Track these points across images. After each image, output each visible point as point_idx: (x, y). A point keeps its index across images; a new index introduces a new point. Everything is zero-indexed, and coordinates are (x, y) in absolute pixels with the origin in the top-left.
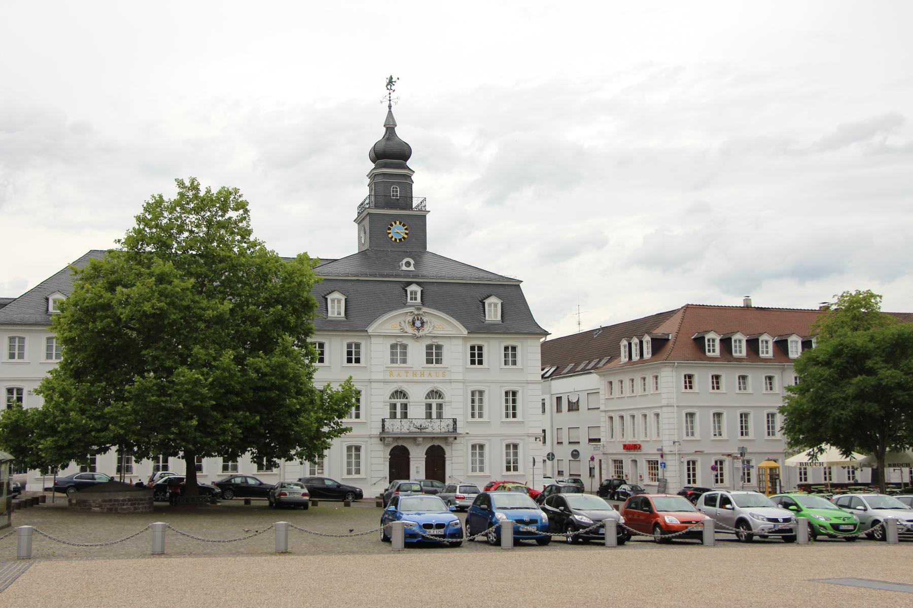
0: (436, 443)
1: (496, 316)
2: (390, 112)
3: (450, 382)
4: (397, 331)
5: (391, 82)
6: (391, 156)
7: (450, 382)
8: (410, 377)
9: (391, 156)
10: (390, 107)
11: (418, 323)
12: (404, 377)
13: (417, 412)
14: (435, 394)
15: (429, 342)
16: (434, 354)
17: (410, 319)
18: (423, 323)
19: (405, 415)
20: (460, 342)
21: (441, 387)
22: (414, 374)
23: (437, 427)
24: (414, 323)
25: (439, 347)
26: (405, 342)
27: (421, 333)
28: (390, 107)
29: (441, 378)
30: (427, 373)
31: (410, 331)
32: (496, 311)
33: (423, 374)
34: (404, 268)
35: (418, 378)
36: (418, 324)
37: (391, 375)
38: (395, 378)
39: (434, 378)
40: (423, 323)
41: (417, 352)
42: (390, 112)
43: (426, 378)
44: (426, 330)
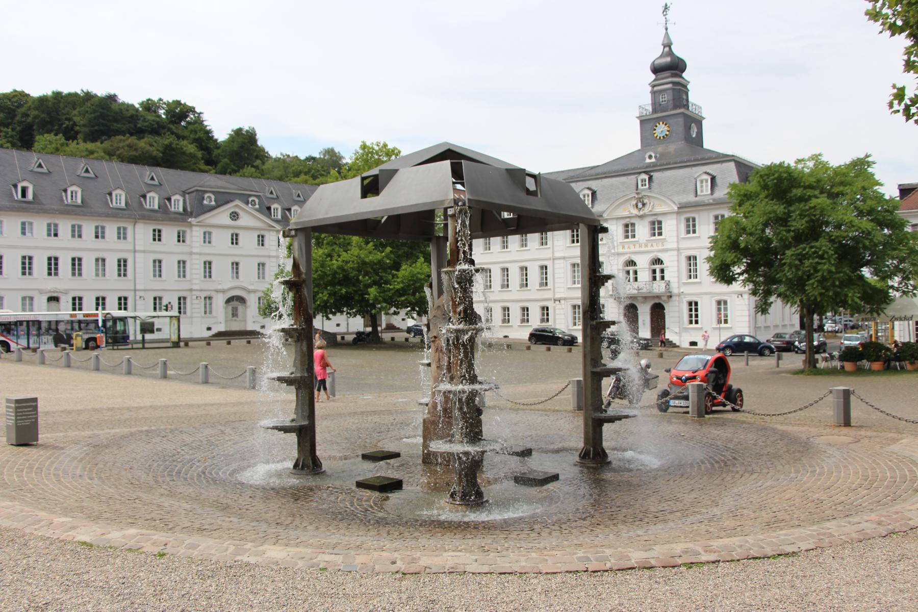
0: (657, 301)
1: (707, 190)
2: (667, 33)
3: (666, 250)
4: (626, 214)
5: (666, 8)
6: (670, 69)
7: (666, 250)
8: (637, 249)
9: (670, 69)
10: (666, 29)
11: (641, 203)
12: (632, 249)
13: (644, 276)
14: (658, 261)
15: (651, 219)
16: (656, 228)
17: (634, 202)
18: (644, 205)
19: (636, 279)
20: (675, 216)
21: (661, 256)
22: (640, 246)
23: (659, 287)
24: (637, 206)
25: (660, 223)
26: (633, 221)
27: (642, 213)
28: (666, 29)
29: (660, 248)
30: (649, 245)
31: (635, 212)
32: (707, 186)
33: (646, 246)
34: (648, 161)
35: (643, 249)
36: (640, 205)
37: (623, 247)
38: (626, 250)
39: (655, 248)
40: (644, 205)
41: (642, 230)
42: (667, 33)
43: (649, 248)
44: (646, 210)
